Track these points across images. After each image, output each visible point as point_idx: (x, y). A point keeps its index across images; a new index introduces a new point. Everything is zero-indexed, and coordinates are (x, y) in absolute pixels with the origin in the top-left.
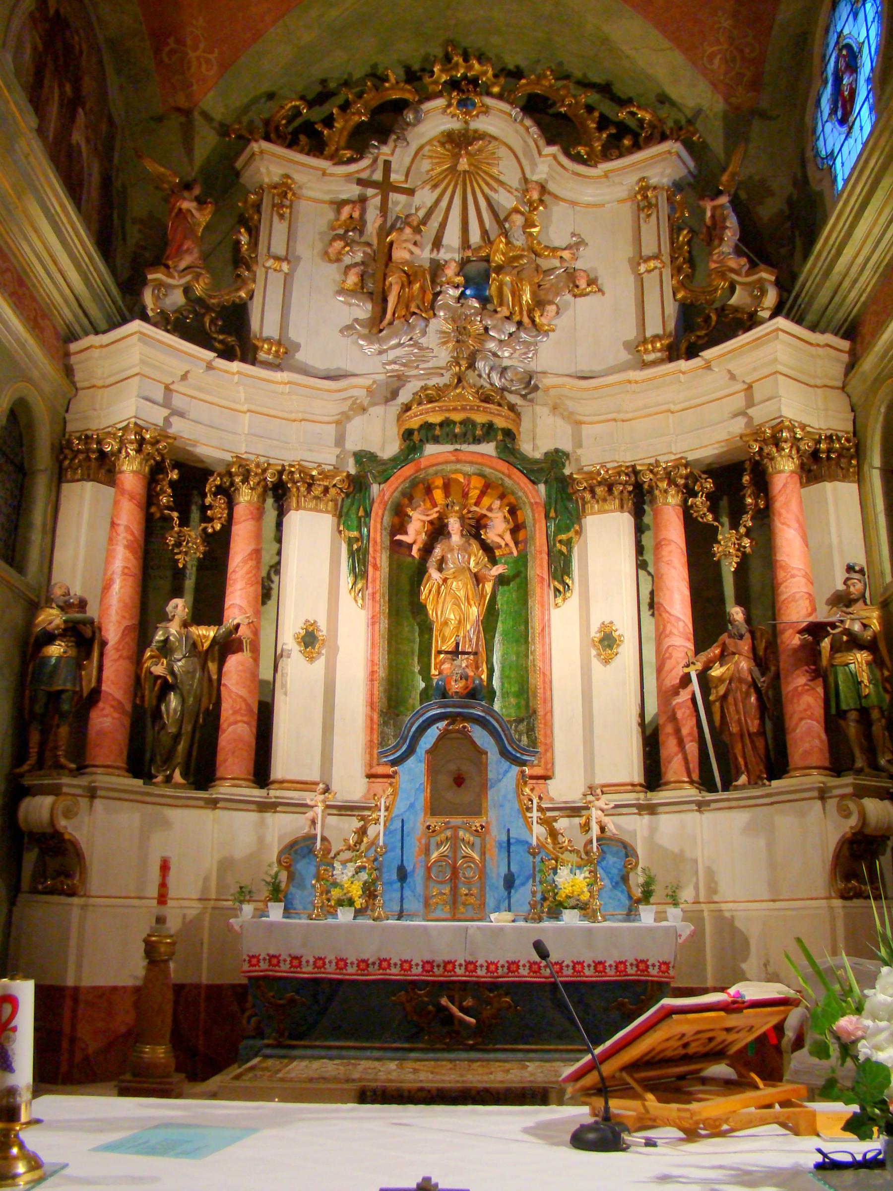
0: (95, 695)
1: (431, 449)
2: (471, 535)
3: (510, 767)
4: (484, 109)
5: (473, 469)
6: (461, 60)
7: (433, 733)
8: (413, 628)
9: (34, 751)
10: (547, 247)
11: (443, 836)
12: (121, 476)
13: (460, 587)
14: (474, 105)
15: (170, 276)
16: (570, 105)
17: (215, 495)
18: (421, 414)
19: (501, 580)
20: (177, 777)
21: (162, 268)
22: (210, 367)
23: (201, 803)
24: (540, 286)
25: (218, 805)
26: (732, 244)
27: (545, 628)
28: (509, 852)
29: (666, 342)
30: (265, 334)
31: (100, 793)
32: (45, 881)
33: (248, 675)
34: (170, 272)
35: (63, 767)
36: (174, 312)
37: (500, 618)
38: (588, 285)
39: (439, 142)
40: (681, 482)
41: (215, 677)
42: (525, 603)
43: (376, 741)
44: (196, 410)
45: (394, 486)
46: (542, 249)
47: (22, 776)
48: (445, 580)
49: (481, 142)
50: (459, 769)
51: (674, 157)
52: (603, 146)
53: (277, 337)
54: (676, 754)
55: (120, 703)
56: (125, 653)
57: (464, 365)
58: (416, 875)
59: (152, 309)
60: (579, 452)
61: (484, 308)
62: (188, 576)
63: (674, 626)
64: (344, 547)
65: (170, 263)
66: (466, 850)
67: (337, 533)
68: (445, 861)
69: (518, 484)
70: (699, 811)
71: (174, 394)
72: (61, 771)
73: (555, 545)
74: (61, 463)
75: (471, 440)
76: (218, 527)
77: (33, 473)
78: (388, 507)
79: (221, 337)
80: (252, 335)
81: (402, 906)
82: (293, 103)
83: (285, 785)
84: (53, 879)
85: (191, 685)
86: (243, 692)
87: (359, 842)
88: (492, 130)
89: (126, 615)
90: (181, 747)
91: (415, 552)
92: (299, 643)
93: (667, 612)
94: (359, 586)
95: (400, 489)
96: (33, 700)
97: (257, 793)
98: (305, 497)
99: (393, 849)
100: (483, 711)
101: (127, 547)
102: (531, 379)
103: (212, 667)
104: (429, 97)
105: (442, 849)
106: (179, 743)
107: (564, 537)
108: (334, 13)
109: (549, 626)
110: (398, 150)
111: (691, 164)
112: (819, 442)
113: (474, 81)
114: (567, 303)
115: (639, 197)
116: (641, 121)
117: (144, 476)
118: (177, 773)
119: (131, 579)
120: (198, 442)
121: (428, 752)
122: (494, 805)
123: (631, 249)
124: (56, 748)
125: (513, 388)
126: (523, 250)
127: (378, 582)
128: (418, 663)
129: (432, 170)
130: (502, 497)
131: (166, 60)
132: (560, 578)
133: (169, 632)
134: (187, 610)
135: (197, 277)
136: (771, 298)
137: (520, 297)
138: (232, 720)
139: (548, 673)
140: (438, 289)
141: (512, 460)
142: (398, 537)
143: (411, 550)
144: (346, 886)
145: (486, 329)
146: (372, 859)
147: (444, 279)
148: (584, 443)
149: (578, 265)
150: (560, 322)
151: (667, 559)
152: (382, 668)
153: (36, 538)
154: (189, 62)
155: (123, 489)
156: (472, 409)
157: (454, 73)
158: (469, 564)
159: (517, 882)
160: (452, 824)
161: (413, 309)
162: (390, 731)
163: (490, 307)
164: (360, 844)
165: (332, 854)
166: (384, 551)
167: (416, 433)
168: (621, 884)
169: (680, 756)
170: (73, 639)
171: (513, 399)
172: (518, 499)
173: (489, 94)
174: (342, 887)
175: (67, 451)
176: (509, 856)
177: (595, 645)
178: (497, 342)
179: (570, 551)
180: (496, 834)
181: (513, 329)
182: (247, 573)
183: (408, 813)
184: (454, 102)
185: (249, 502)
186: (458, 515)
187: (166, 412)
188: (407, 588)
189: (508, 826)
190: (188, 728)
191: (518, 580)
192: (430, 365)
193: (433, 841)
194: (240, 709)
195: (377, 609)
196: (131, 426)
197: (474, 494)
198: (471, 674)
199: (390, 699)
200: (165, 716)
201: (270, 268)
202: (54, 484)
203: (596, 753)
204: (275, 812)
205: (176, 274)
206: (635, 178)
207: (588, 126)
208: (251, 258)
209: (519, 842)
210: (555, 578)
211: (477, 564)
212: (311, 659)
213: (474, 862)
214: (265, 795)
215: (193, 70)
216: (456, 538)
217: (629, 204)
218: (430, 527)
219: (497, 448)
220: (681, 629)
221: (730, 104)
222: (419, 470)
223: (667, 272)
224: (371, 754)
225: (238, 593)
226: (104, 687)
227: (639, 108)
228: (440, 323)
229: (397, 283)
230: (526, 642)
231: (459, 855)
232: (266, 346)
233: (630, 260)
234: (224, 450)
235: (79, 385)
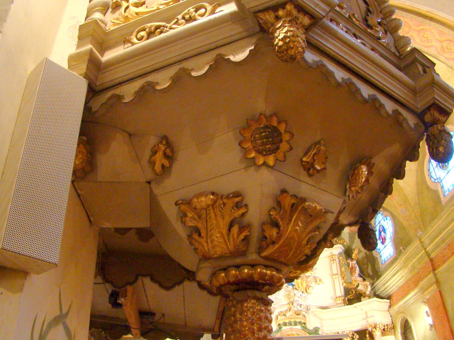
1: (284, 328)
26: (358, 274)
29: (343, 298)
38: (320, 281)
40: (351, 336)
51: (340, 248)
61: (293, 288)
111: (343, 248)
112: (384, 326)
115: (331, 257)
136: (369, 288)
141: (305, 330)
149: (316, 275)
163: (294, 287)
181: (301, 293)
217: (327, 258)
221: (350, 230)
223: (340, 278)
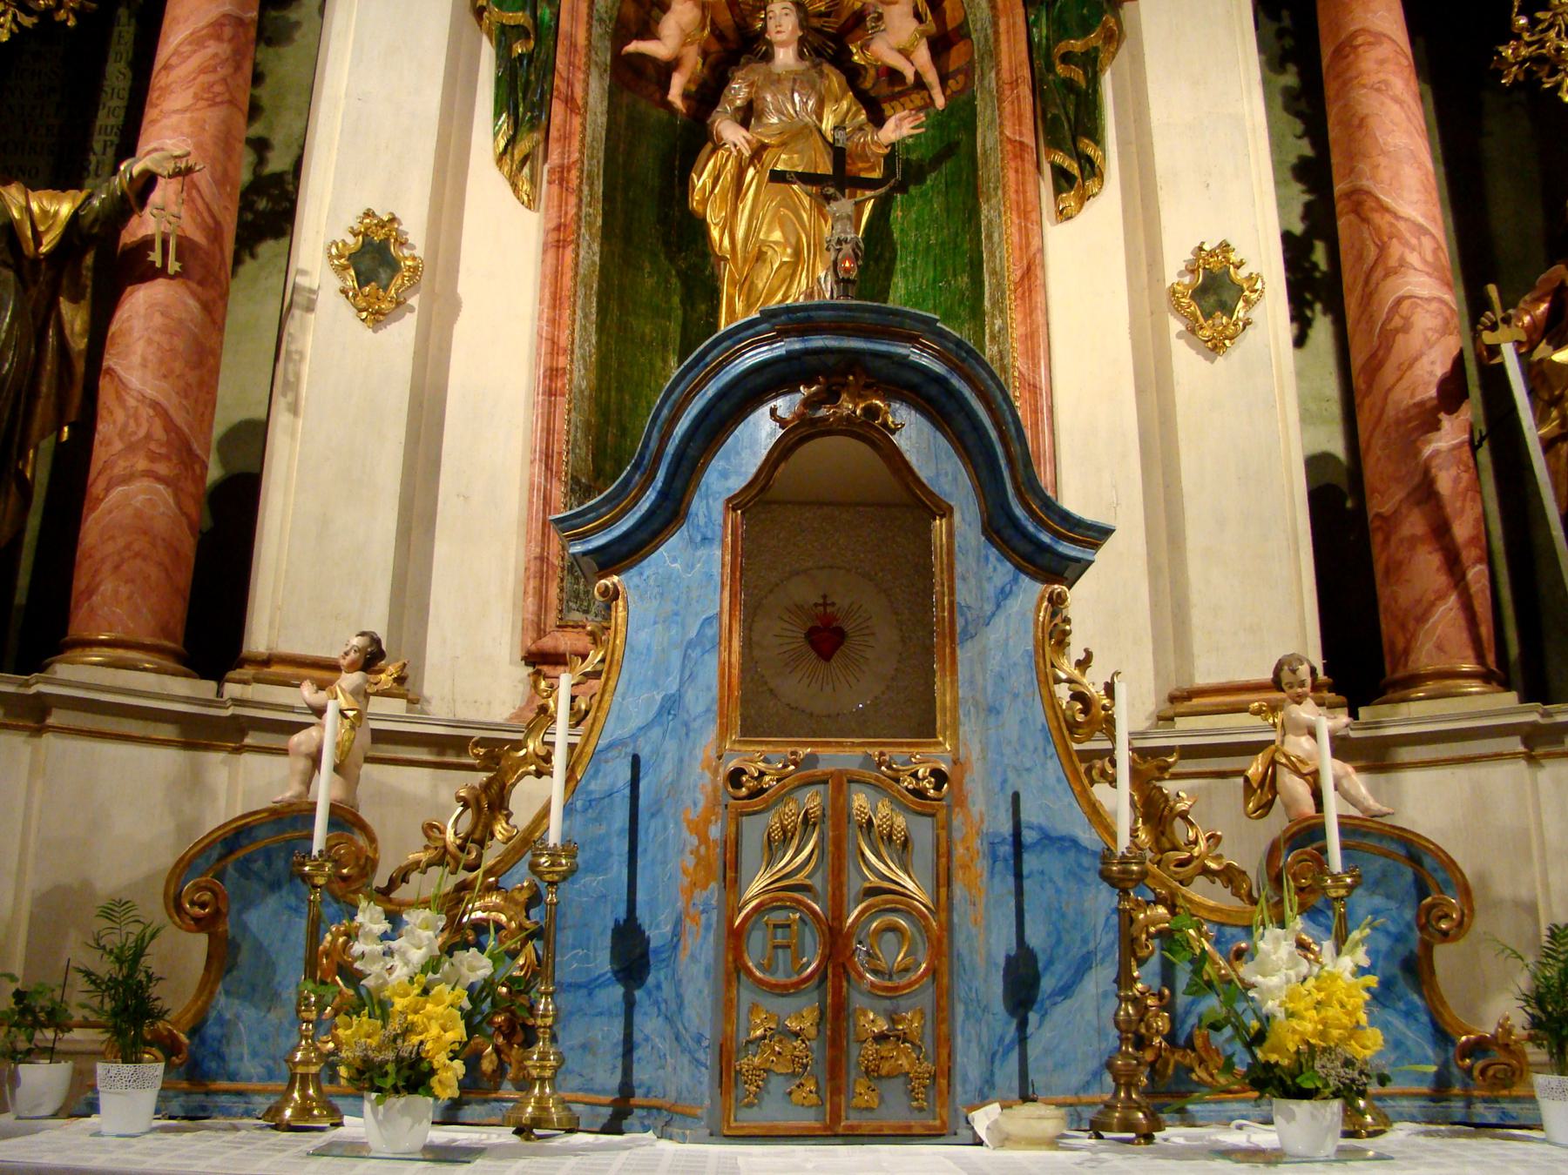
3: (1015, 580)
8: (667, 281)
11: (790, 812)
25: (51, 721)
27: (1031, 273)
28: (1019, 876)
33: (180, 344)
37: (899, 266)
41: (79, 344)
42: (973, 214)
48: (759, 151)
54: (1441, 597)
58: (683, 957)
62: (92, 168)
63: (1406, 244)
64: (487, 53)
66: (880, 866)
67: (471, 19)
70: (1531, 759)
73: (1050, 68)
81: (627, 1071)
83: (276, 669)
87: (479, 836)
93: (1385, 209)
94: (524, 146)
99: (597, 866)
100: (940, 356)
105: (788, 860)
107: (1077, 45)
121: (734, 503)
122: (976, 705)
132: (1069, 141)
138: (120, 467)
142: (635, 46)
143: (666, 87)
144: (399, 1004)
146: (523, 897)
151: (1374, 79)
159: (1047, 984)
160: (822, 768)
164: (481, 844)
165: (380, 880)
166: (594, 72)
168: (1402, 985)
169: (1453, 598)
174: (383, 1009)
176: (1019, 892)
177: (1178, 308)
179: (1094, 81)
182: (203, 70)
183: (656, 732)
189: (1014, 782)
191: (947, 167)
193: (754, 832)
194: (148, 437)
195: (572, 211)
203: (1194, 597)
204: (238, 750)
209: (1049, 840)
210: (1055, 143)
212: (377, 318)
213: (909, 913)
214: (212, 696)
216: (785, 57)
218: (715, 47)
220: (1430, 258)
224: (541, 597)
231: (854, 886)
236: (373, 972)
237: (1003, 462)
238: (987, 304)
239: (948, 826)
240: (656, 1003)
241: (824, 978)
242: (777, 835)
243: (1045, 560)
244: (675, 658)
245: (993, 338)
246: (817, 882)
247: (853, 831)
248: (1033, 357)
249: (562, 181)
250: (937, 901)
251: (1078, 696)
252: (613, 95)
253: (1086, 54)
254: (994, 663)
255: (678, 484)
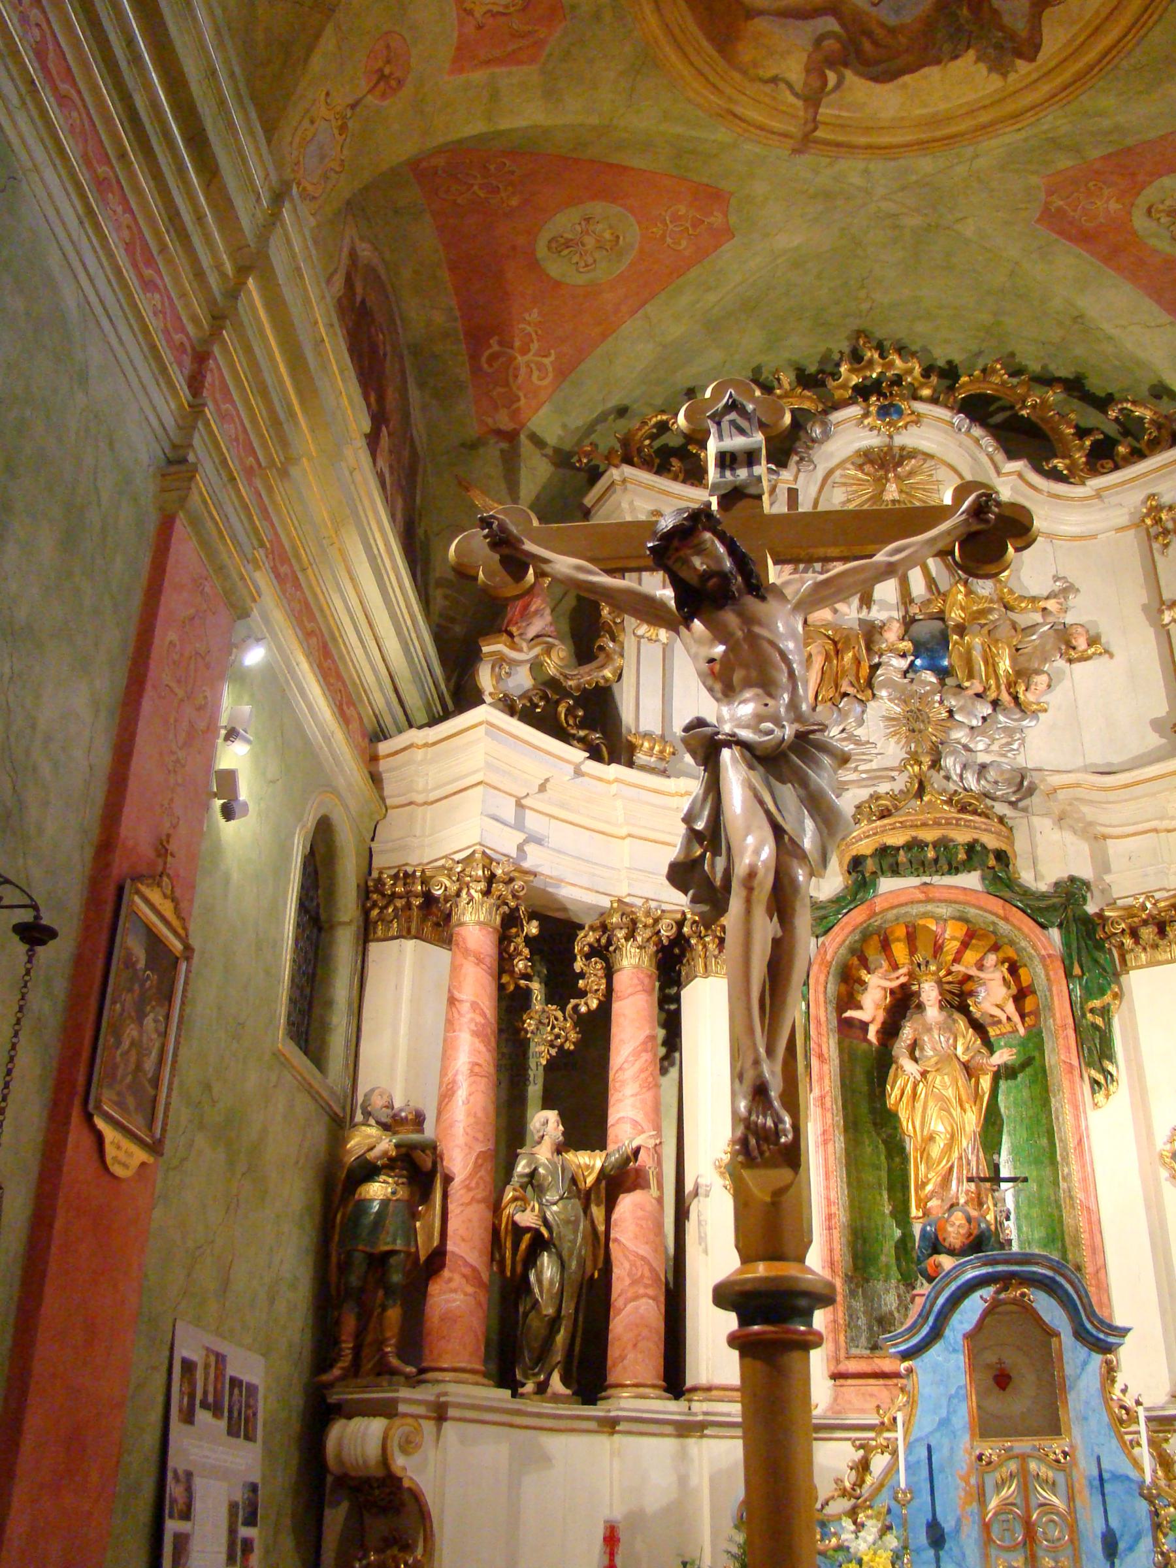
0: (438, 1259)
1: (887, 884)
2: (952, 1006)
4: (913, 418)
5: (950, 909)
6: (876, 356)
7: (974, 1306)
8: (877, 1147)
9: (347, 1346)
10: (1022, 598)
11: (1005, 1471)
12: (463, 931)
13: (946, 1084)
14: (900, 413)
15: (514, 647)
16: (1034, 406)
17: (588, 957)
18: (875, 834)
19: (1006, 1073)
20: (556, 1384)
21: (505, 637)
22: (578, 773)
23: (593, 1425)
24: (1017, 650)
28: (1103, 1495)
30: (643, 728)
31: (451, 1412)
32: (366, 1556)
34: (514, 642)
35: (394, 1372)
36: (520, 697)
38: (1090, 645)
39: (853, 463)
41: (601, 1228)
42: (1045, 1103)
43: (841, 1322)
44: (558, 834)
45: (839, 939)
46: (1016, 599)
47: (330, 1385)
48: (924, 1074)
49: (913, 461)
50: (1000, 1362)
52: (1088, 456)
53: (659, 732)
55: (474, 1269)
56: (480, 1194)
57: (927, 760)
58: (963, 1535)
59: (491, 694)
60: (1108, 878)
62: (531, 1079)
65: (514, 629)
68: (1011, 1512)
69: (1019, 929)
71: (527, 811)
72: (395, 1378)
73: (1084, 1016)
74: (366, 913)
75: (946, 868)
76: (594, 1004)
77: (332, 927)
78: (833, 968)
79: (582, 733)
80: (624, 730)
82: (659, 418)
83: (714, 1393)
84: (378, 1551)
85: (574, 1241)
86: (644, 1250)
88: (926, 445)
89: (480, 1136)
90: (561, 1338)
91: (872, 1035)
92: (722, 1174)
95: (847, 942)
96: (345, 1267)
97: (672, 1408)
98: (716, 957)
101: (475, 1034)
102: (1023, 778)
103: (598, 1212)
104: (836, 407)
106: (559, 1331)
107: (1096, 1003)
108: (712, 297)
109: (1088, 1137)
110: (802, 476)
113: (898, 381)
114: (1061, 672)
115: (1148, 521)
116: (1141, 419)
117: (495, 929)
118: (556, 1380)
119: (484, 1080)
120: (562, 881)
121: (968, 1336)
123: (1144, 592)
124: (381, 1343)
125: (999, 793)
126: (992, 601)
127: (827, 1081)
128: (889, 1198)
129: (849, 501)
130: (995, 948)
131: (485, 366)
133: (537, 1159)
134: (561, 1128)
135: (548, 650)
137: (995, 666)
138: (630, 1294)
139: (1094, 1207)
140: (876, 660)
141: (1007, 894)
142: (849, 1014)
143: (866, 1031)
144: (865, 1559)
145: (951, 712)
147: (884, 646)
148: (1114, 867)
149: (1069, 619)
150: (1053, 699)
152: (842, 1209)
153: (339, 1020)
154: (517, 369)
155: (467, 950)
156: (948, 823)
157: (868, 374)
158: (955, 1049)
160: (1016, 1451)
161: (845, 687)
162: (858, 1305)
163: (949, 681)
164: (860, 1486)
167: (869, 862)
170: (405, 1172)
171: (1001, 809)
172: (1018, 951)
173: (916, 397)
175: (375, 896)
177: (1164, 1164)
178: (967, 730)
179: (1109, 1024)
180: (1085, 1467)
181: (987, 710)
182: (642, 1071)
183: (938, 1435)
184: (873, 409)
185: (637, 967)
186: (934, 977)
187: (520, 837)
188: (865, 1089)
190: (568, 1308)
191: (1029, 1070)
192: (874, 765)
194: (642, 1276)
195: (829, 1121)
196: (478, 856)
197: (952, 946)
198: (974, 1213)
199: (855, 1257)
200: (536, 1290)
201: (642, 637)
202: (361, 942)
204: (703, 1436)
205: (524, 645)
206: (1142, 496)
207: (1061, 433)
208: (615, 623)
211: (967, 1049)
213: (1058, 1514)
214: (686, 1410)
215: (520, 379)
216: (933, 1013)
217: (1132, 532)
219: (983, 878)
222: (873, 914)
225: (629, 1101)
226: (450, 1247)
227: (1134, 403)
228: (884, 705)
229: (819, 653)
230: (1053, 1163)
231: (1033, 1503)
232: (646, 744)
233: (1145, 608)
234: (597, 892)
235: (389, 802)
236: (853, 1546)
237: (1080, 1307)
238: (1059, 1158)
239: (1070, 1475)
240: (951, 1557)
241: (1025, 1544)
242: (1000, 1482)
243: (1101, 1344)
244: (944, 1401)
245: (1064, 1178)
246: (1018, 1501)
247: (1030, 1479)
248: (1086, 1190)
249: (823, 1105)
250: (1069, 1507)
251: (1123, 1407)
252: (840, 1043)
253: (1103, 1007)
254: (1083, 1397)
255: (939, 1323)
